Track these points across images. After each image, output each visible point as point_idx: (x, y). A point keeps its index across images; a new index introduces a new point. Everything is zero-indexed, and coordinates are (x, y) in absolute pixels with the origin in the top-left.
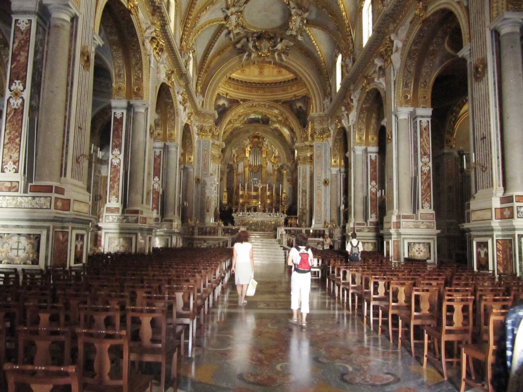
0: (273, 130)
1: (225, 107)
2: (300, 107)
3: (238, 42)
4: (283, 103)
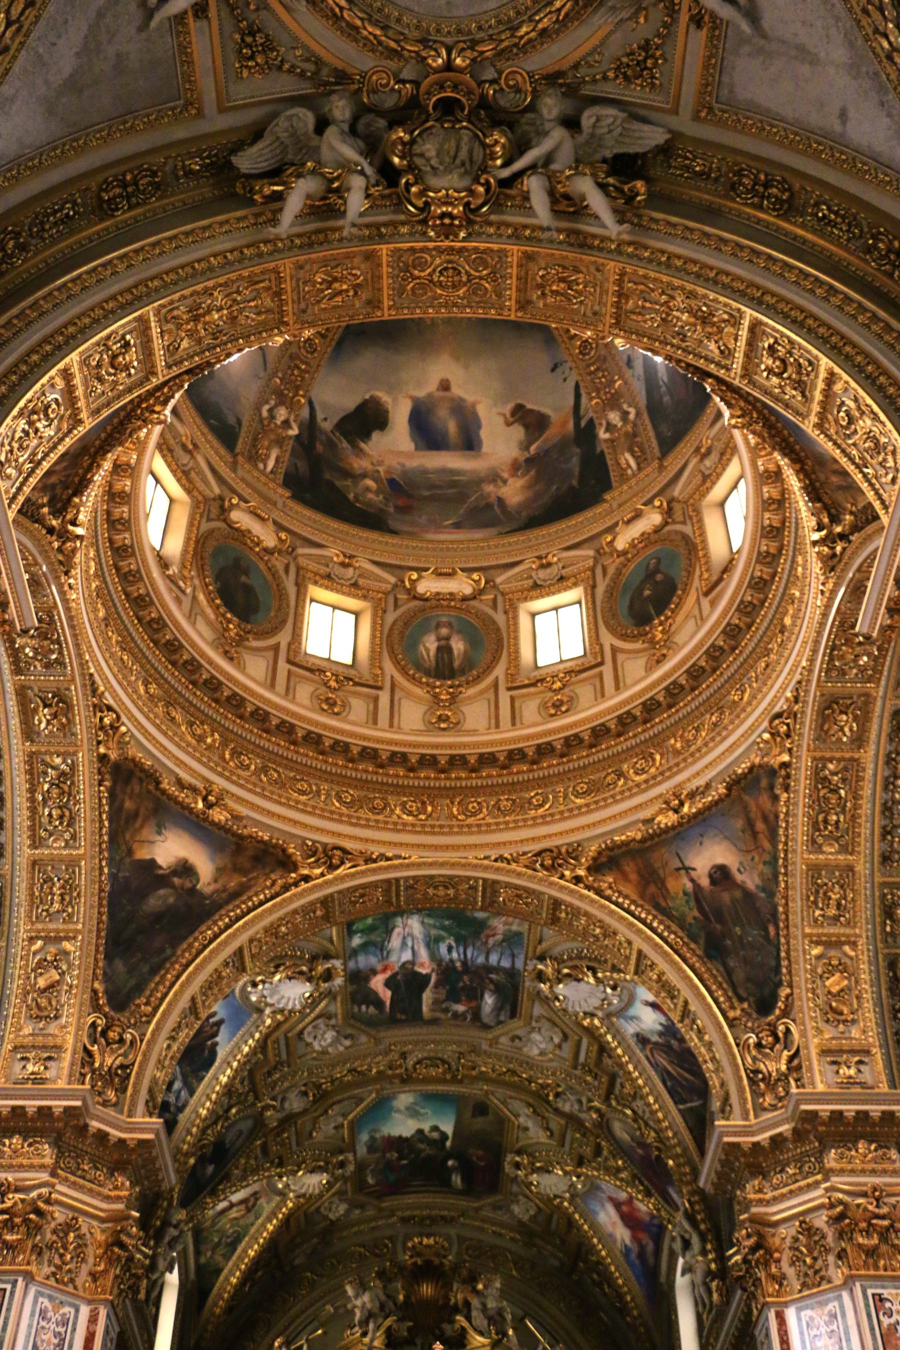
0: (527, 1232)
1: (193, 891)
2: (721, 875)
3: (257, 134)
4: (595, 868)
